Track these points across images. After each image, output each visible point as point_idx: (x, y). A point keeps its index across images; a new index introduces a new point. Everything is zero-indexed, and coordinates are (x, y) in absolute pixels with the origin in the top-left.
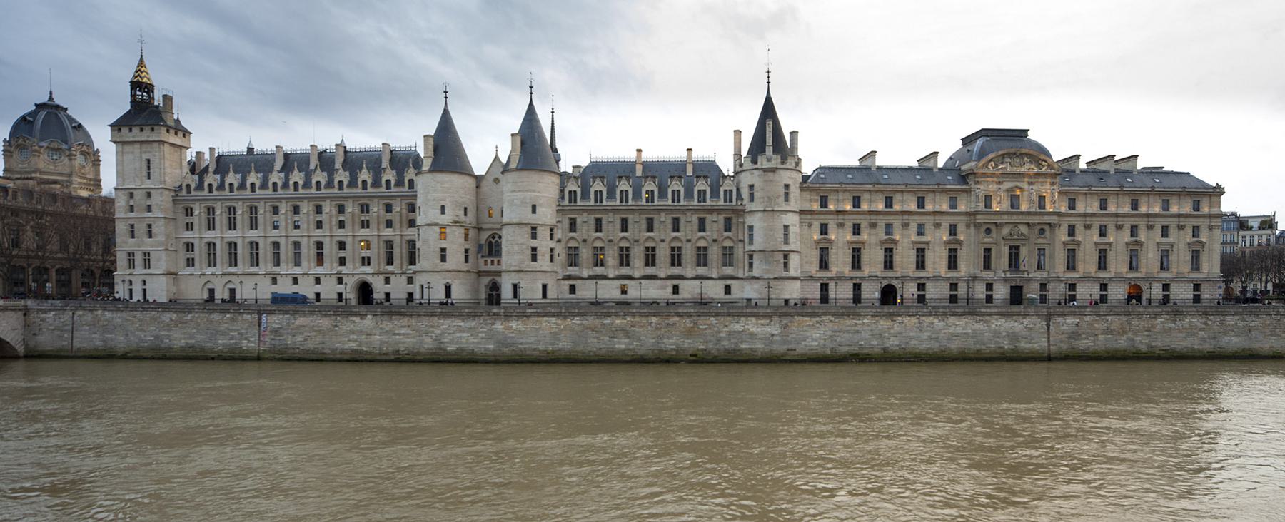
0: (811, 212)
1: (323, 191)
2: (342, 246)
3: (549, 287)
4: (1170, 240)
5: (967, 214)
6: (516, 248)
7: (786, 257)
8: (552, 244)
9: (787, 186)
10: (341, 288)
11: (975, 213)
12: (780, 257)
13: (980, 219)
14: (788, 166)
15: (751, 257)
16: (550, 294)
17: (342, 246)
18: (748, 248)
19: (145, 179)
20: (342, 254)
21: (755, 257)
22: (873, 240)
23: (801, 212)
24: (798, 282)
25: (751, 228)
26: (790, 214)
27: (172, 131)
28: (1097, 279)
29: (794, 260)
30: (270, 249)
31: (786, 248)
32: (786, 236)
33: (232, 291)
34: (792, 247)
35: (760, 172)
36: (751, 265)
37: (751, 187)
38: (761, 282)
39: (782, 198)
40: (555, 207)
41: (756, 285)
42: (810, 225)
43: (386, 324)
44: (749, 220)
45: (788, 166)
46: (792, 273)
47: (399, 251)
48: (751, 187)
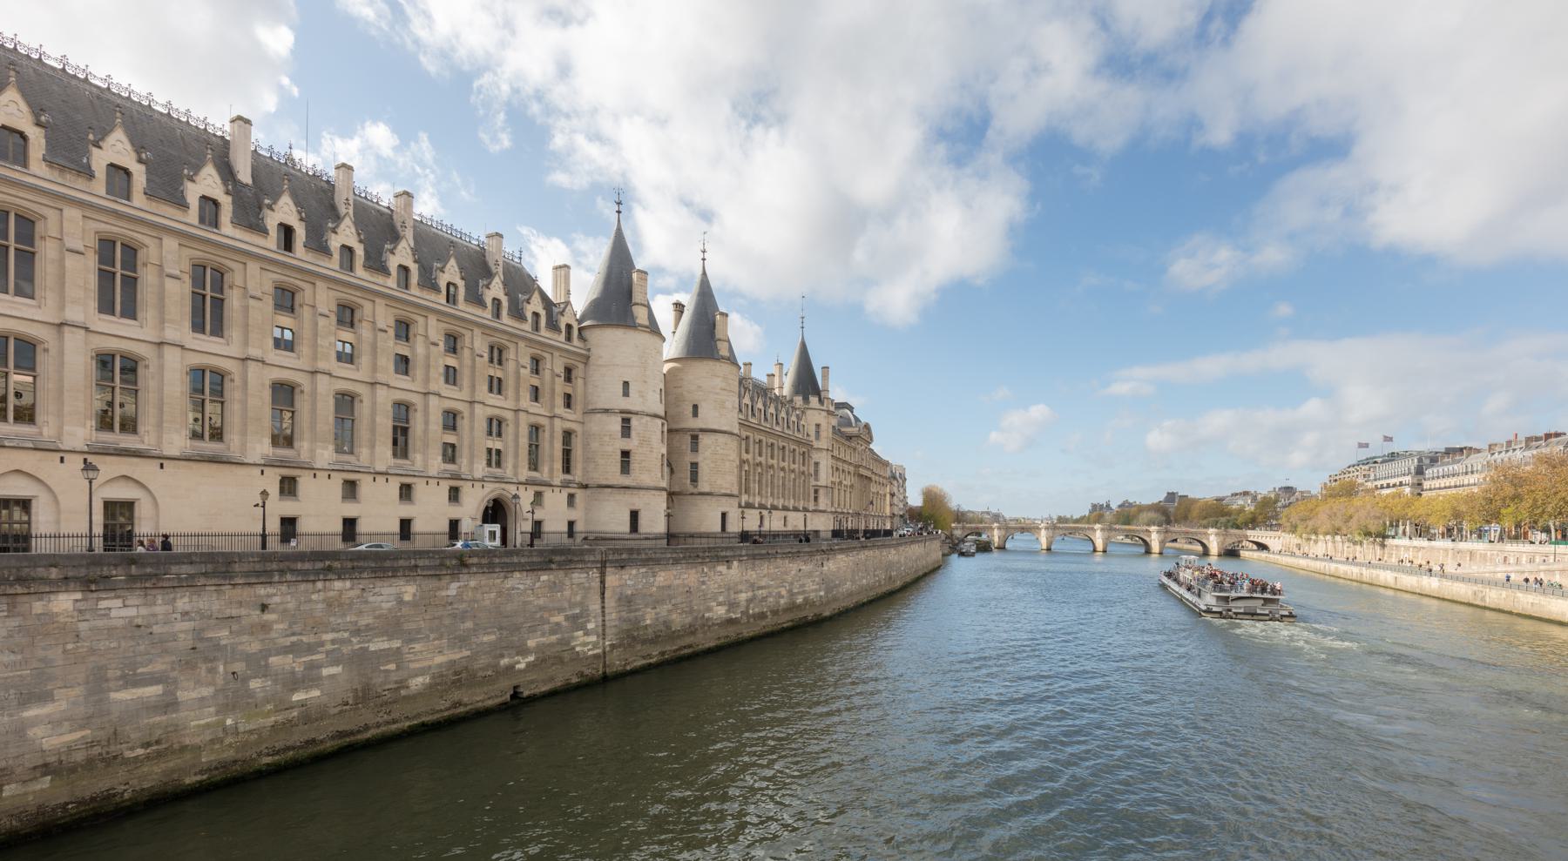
2: (451, 420)
10: (455, 512)
13: (863, 471)
15: (816, 492)
17: (451, 420)
18: (813, 483)
20: (496, 444)
21: (821, 492)
25: (817, 464)
30: (327, 408)
33: (119, 511)
37: (818, 426)
43: (752, 575)
44: (816, 456)
47: (552, 449)
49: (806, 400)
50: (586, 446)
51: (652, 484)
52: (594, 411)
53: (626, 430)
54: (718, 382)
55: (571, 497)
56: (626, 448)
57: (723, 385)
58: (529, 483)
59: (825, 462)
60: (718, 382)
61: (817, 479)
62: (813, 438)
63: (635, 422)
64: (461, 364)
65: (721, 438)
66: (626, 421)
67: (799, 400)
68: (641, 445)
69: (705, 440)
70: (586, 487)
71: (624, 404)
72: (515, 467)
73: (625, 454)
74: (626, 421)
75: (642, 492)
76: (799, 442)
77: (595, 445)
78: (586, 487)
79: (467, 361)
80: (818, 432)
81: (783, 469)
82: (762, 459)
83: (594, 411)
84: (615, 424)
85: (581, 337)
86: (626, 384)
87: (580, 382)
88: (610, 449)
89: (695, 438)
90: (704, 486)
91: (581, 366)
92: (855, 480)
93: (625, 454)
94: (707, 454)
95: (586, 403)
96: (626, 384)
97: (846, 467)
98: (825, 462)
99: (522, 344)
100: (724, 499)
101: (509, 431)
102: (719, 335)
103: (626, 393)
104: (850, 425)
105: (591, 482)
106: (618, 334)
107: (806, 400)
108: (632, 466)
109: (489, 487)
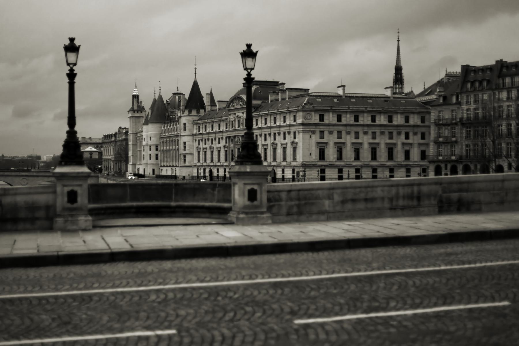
0: (196, 135)
3: (155, 170)
4: (286, 141)
7: (185, 156)
8: (157, 152)
9: (185, 124)
12: (182, 156)
14: (185, 114)
16: (156, 173)
22: (208, 148)
23: (193, 135)
24: (190, 169)
26: (186, 137)
27: (136, 112)
28: (371, 166)
29: (188, 158)
31: (184, 152)
32: (185, 147)
34: (187, 152)
39: (182, 130)
40: (158, 137)
42: (196, 140)
45: (185, 114)
46: (187, 164)
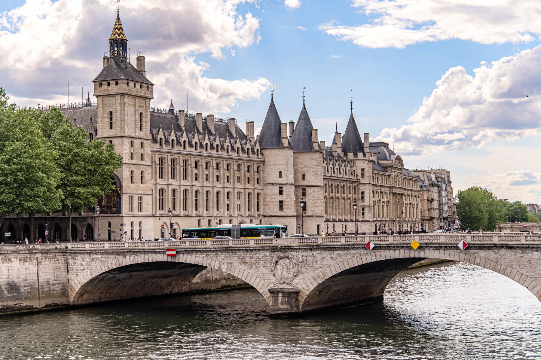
1: (220, 153)
5: (391, 188)
6: (319, 201)
11: (393, 187)
13: (395, 191)
15: (363, 209)
19: (138, 130)
21: (366, 209)
25: (363, 193)
35: (366, 162)
36: (363, 214)
37: (363, 170)
38: (369, 223)
41: (368, 225)
44: (362, 188)
48: (363, 170)
49: (356, 155)
50: (265, 199)
51: (292, 214)
52: (267, 184)
53: (281, 193)
54: (314, 163)
55: (260, 220)
56: (282, 200)
57: (317, 164)
58: (249, 216)
59: (368, 191)
60: (314, 163)
61: (363, 202)
62: (360, 177)
63: (284, 188)
64: (230, 174)
65: (316, 189)
66: (281, 188)
67: (351, 155)
68: (287, 198)
69: (309, 191)
70: (265, 216)
71: (280, 181)
72: (245, 210)
73: (281, 202)
74: (281, 188)
75: (288, 218)
76: (352, 182)
77: (268, 199)
78: (265, 216)
79: (232, 173)
80: (363, 174)
81: (344, 198)
82: (333, 195)
83: (267, 184)
84: (277, 190)
85: (262, 154)
86: (280, 172)
87: (262, 172)
88: (275, 200)
89: (304, 189)
90: (309, 213)
91: (262, 165)
92: (390, 197)
93: (281, 202)
94: (310, 197)
95: (264, 181)
96: (280, 172)
97: (383, 189)
98: (368, 191)
99: (245, 162)
100: (318, 219)
101: (242, 196)
102: (313, 139)
103: (281, 176)
104: (386, 159)
105: (267, 214)
106: (277, 151)
107: (356, 155)
108: (284, 207)
109: (239, 219)
